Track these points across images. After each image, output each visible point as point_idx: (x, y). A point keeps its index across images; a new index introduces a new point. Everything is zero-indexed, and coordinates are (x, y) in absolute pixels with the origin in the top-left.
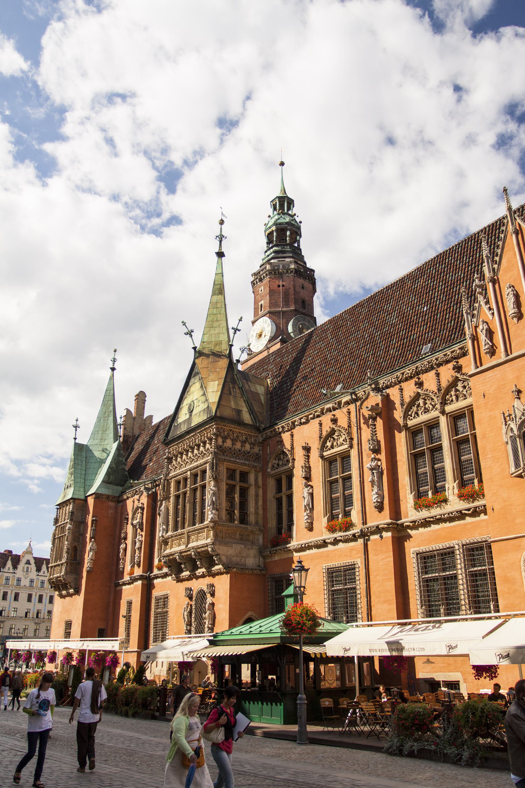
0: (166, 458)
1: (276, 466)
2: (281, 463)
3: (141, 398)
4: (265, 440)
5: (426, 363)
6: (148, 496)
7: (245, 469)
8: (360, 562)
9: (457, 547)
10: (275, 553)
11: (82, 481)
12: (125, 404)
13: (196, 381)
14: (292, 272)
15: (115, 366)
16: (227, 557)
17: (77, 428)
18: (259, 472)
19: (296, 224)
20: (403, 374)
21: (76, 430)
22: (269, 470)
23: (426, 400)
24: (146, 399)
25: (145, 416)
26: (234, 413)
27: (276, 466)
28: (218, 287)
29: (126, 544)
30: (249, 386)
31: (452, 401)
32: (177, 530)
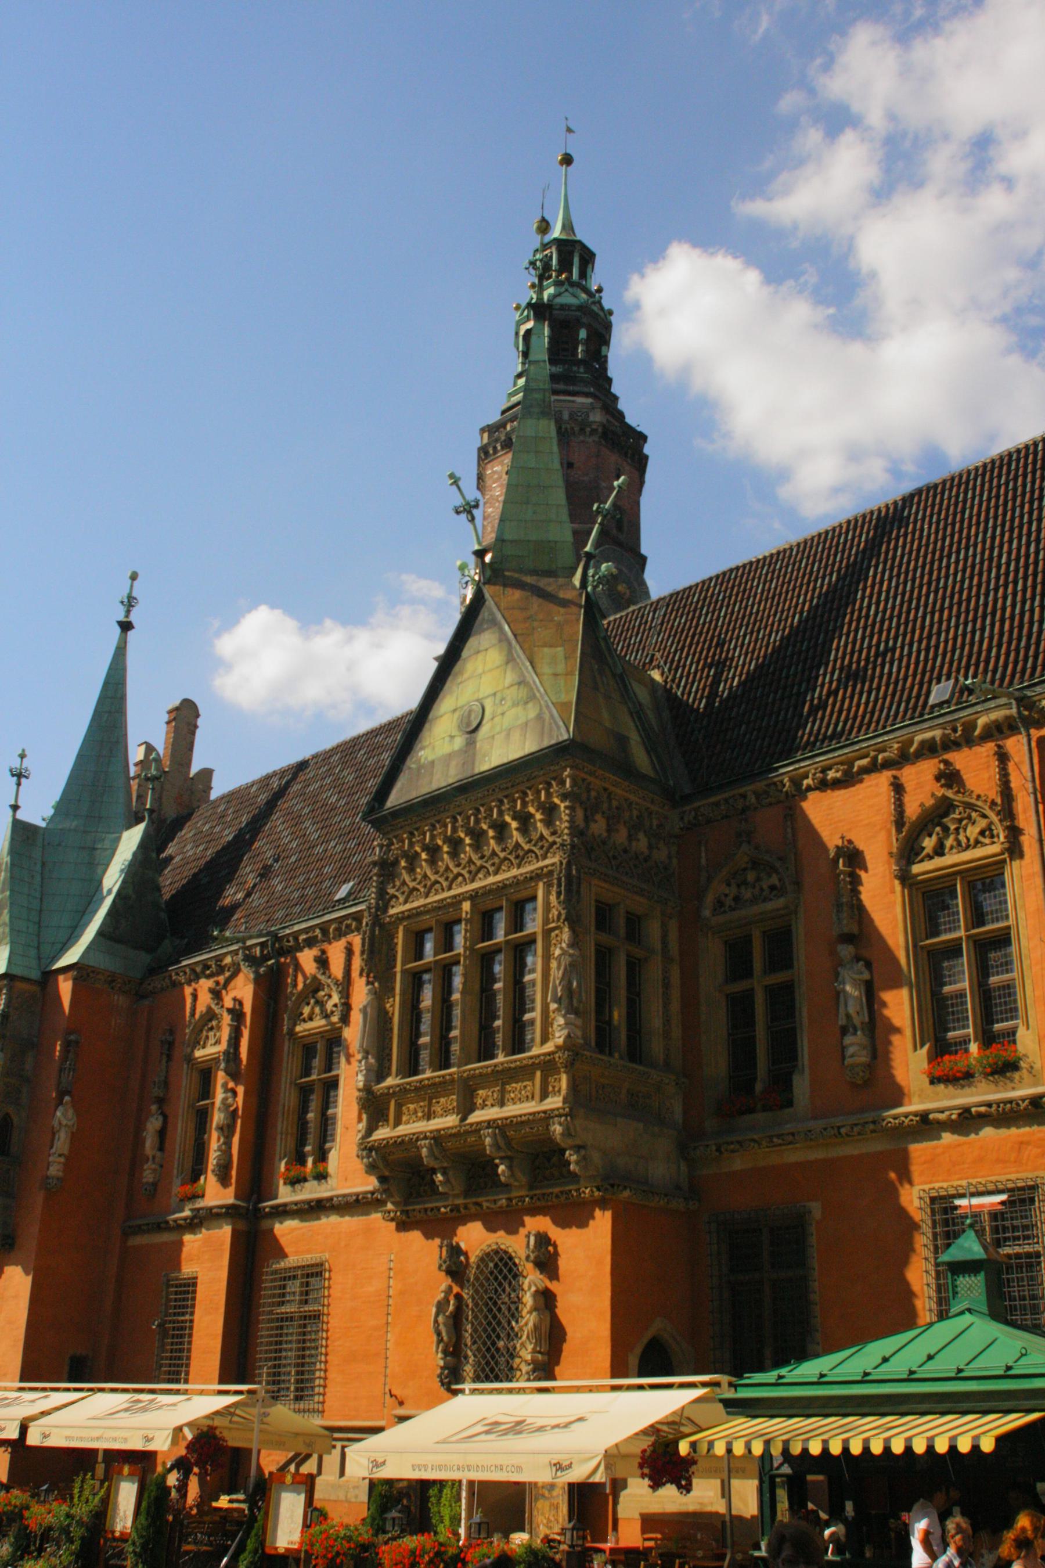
0: (375, 864)
1: (729, 902)
2: (747, 894)
6: (258, 981)
10: (733, 1151)
14: (593, 432)
15: (133, 618)
17: (23, 780)
19: (601, 313)
21: (19, 784)
22: (707, 913)
24: (200, 722)
25: (194, 769)
27: (729, 902)
29: (165, 1117)
32: (415, 1072)
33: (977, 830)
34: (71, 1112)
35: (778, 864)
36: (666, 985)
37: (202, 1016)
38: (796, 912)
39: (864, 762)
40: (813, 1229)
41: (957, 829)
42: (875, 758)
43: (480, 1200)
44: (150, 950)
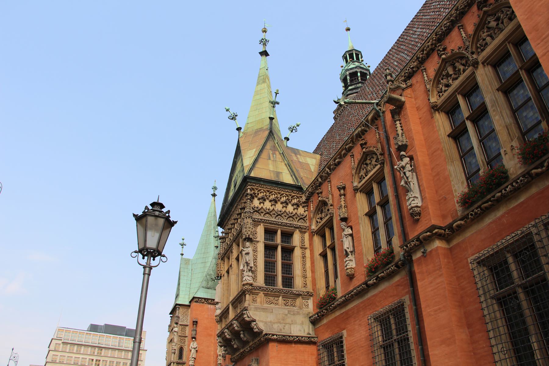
1: (319, 220)
8: (407, 300)
9: (534, 231)
11: (188, 289)
18: (305, 232)
26: (272, 175)
28: (262, 77)
30: (297, 158)
31: (486, 44)
36: (304, 257)
40: (344, 342)
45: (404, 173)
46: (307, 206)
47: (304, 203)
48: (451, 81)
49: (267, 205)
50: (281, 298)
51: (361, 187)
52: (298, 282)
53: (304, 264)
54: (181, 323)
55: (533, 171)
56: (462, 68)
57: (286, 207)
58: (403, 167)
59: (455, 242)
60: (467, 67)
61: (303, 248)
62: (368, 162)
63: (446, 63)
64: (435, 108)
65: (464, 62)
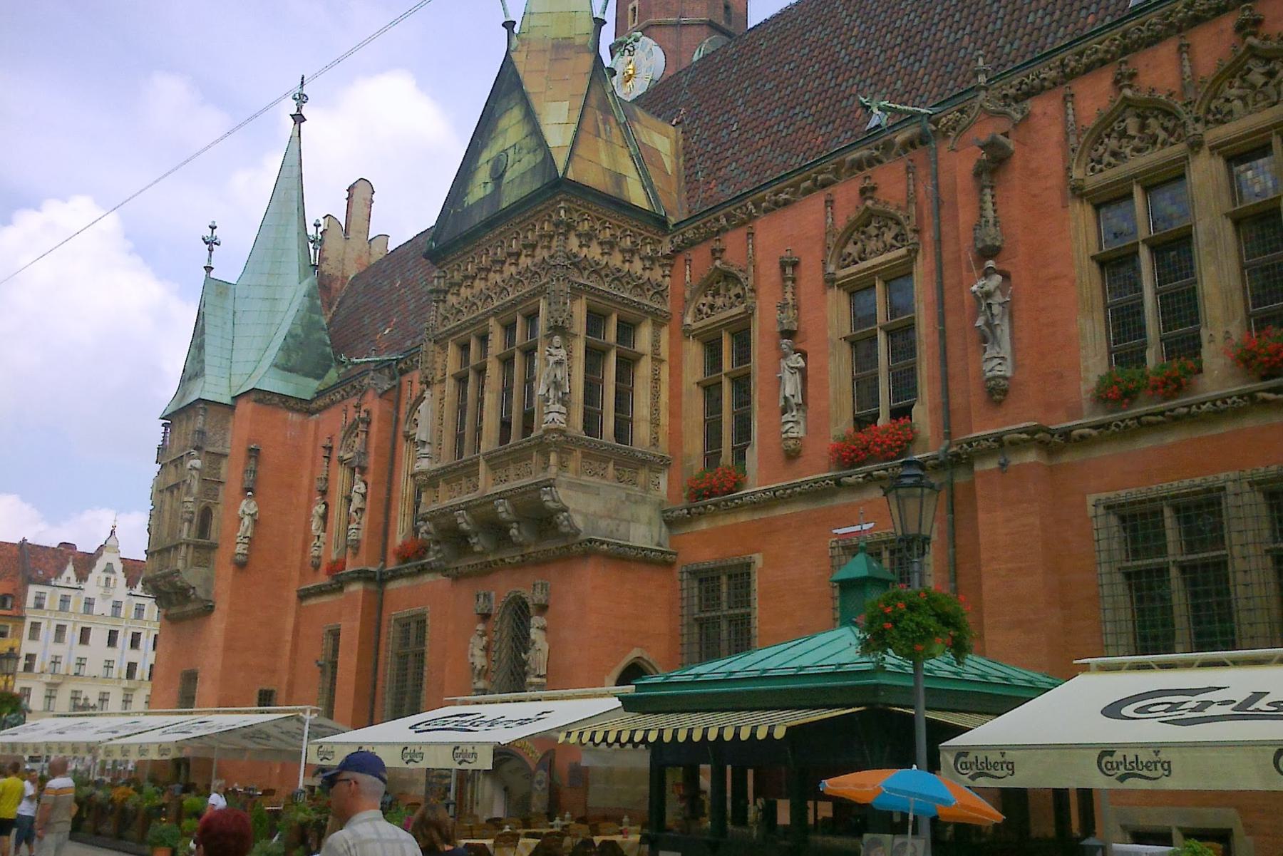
1: (705, 309)
3: (360, 194)
4: (676, 252)
5: (1154, 20)
7: (631, 314)
9: (1230, 487)
12: (324, 202)
13: (513, 104)
16: (586, 515)
18: (662, 325)
20: (1081, 54)
21: (211, 250)
22: (688, 320)
23: (1147, 118)
29: (327, 506)
31: (1230, 112)
33: (892, 234)
34: (253, 504)
35: (741, 275)
36: (656, 380)
37: (350, 427)
38: (752, 314)
39: (808, 183)
41: (877, 236)
42: (816, 179)
43: (503, 556)
44: (319, 377)
45: (989, 306)
46: (672, 266)
47: (667, 257)
48: (1128, 151)
49: (594, 252)
50: (611, 465)
51: (844, 277)
52: (642, 432)
53: (656, 395)
54: (211, 449)
55: (1260, 395)
56: (1162, 135)
57: (631, 262)
58: (988, 295)
59: (1065, 459)
60: (1172, 140)
61: (657, 359)
62: (872, 230)
63: (1129, 106)
64: (1078, 192)
65: (1170, 125)
